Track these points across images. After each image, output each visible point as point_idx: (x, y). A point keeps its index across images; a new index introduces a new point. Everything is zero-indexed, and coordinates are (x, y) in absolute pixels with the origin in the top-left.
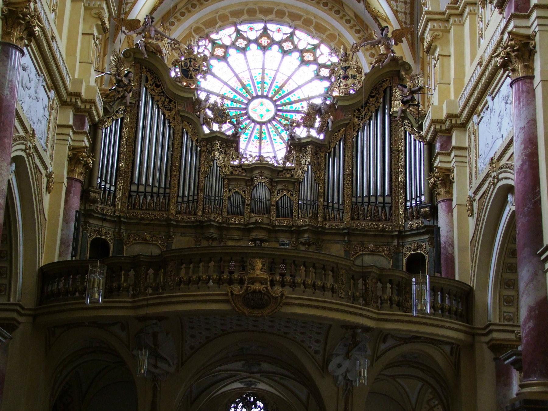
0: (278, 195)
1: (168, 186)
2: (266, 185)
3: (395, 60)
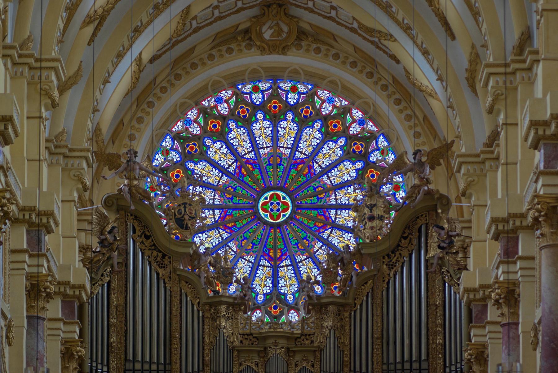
0: (296, 367)
1: (168, 361)
2: (282, 357)
3: (429, 193)
